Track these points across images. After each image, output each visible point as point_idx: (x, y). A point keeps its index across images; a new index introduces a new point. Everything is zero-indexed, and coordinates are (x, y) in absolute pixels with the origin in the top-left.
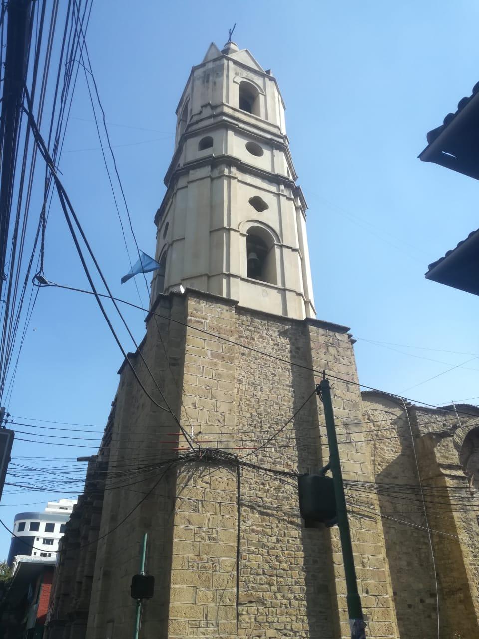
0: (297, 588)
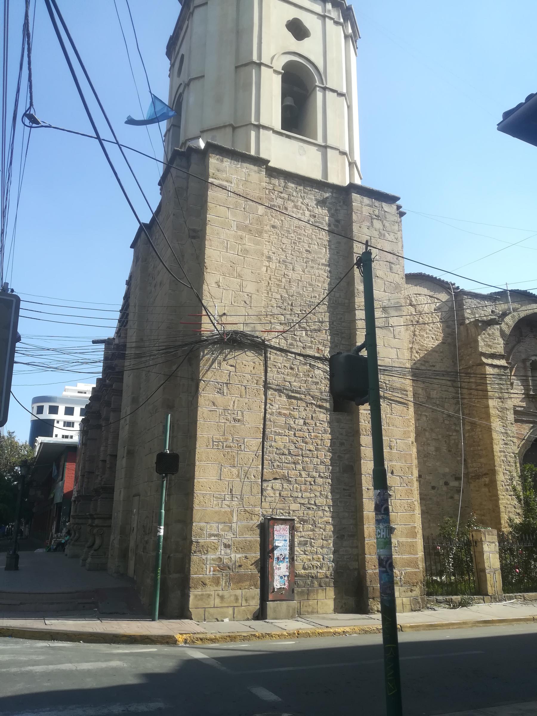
0: (322, 468)
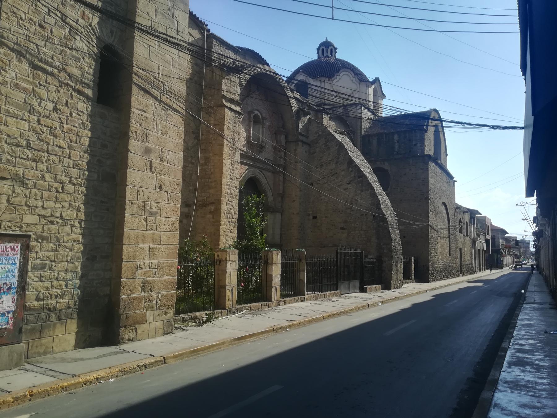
0: (75, 172)
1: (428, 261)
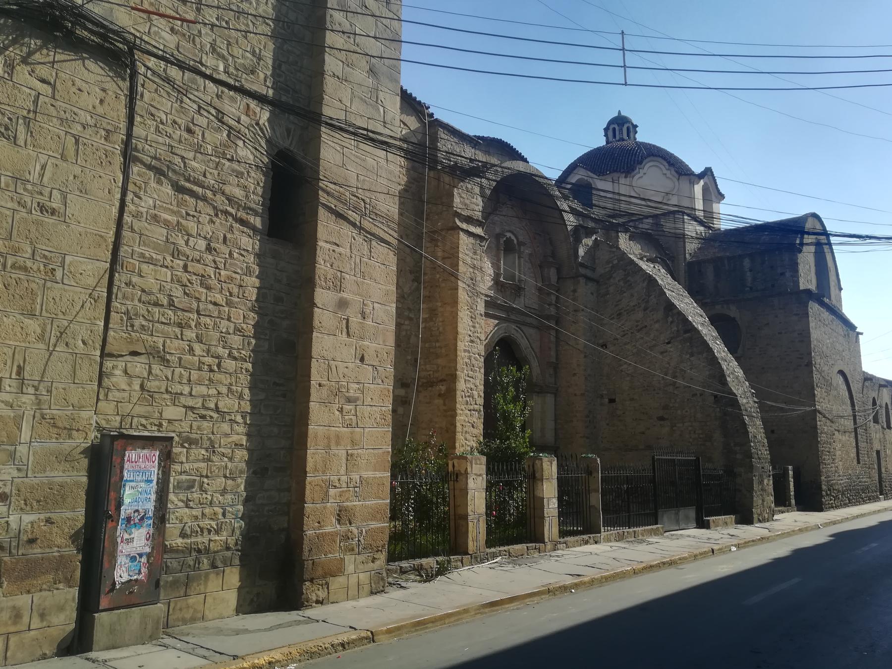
0: (236, 340)
1: (818, 473)
